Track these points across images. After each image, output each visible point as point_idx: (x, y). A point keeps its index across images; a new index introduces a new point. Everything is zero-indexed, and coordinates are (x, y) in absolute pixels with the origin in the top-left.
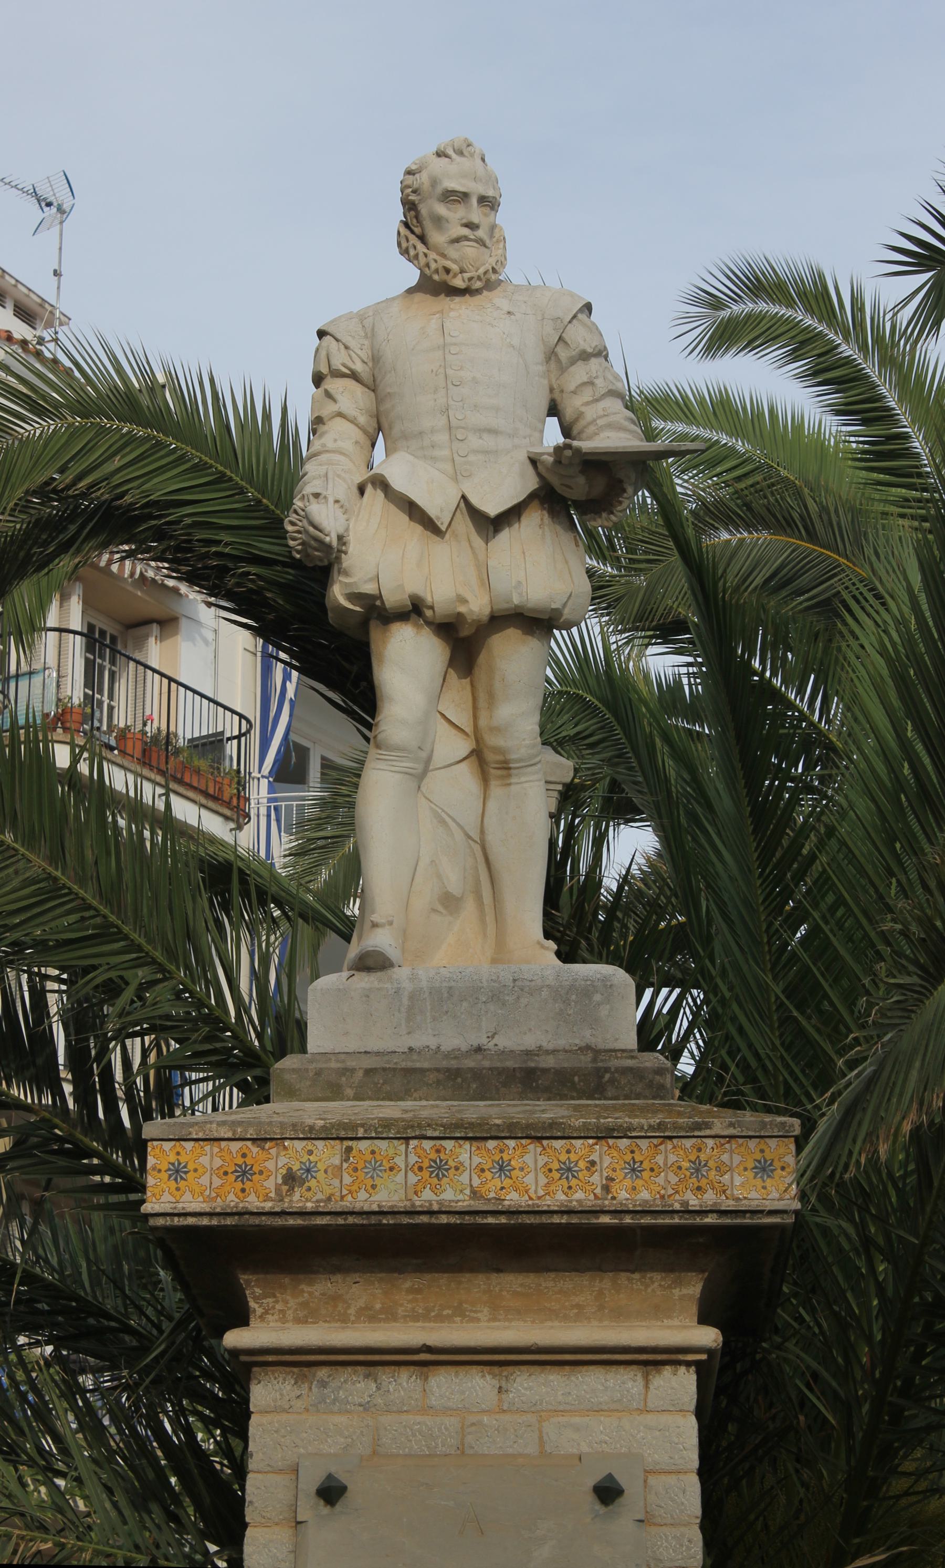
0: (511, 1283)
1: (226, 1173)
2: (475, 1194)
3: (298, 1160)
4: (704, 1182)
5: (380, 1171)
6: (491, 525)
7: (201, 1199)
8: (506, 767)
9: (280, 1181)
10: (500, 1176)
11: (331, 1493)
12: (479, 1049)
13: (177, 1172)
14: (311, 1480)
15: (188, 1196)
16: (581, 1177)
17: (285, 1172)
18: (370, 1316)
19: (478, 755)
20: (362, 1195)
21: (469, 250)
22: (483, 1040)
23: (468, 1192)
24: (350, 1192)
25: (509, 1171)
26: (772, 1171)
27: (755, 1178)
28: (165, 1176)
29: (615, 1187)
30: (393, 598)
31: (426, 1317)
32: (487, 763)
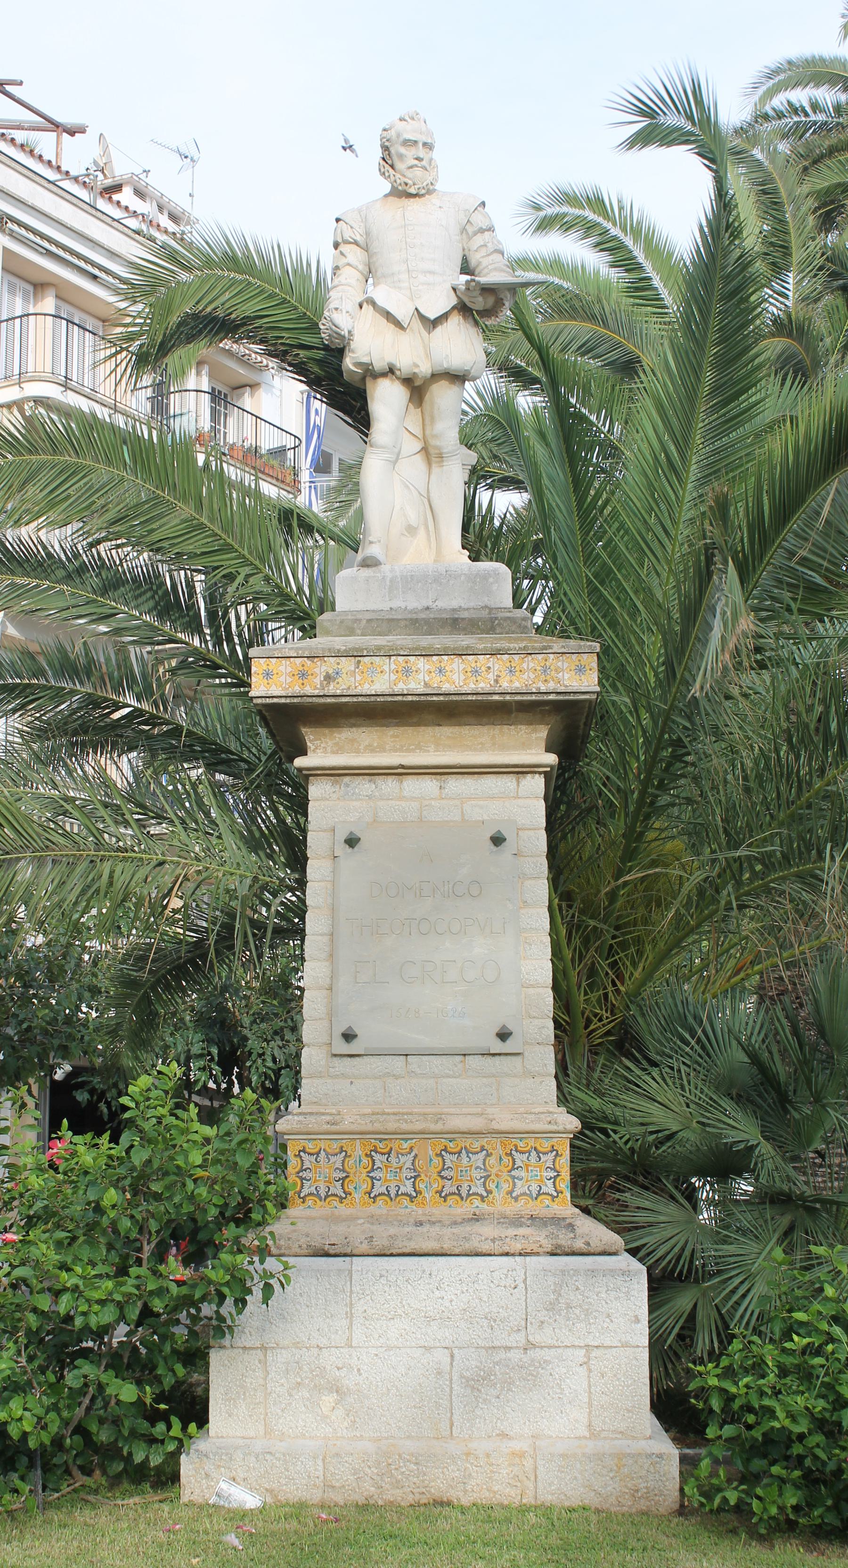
0: (447, 731)
4: (548, 677)
6: (433, 324)
8: (440, 456)
11: (352, 842)
12: (428, 608)
13: (268, 675)
14: (342, 835)
15: (274, 688)
18: (371, 749)
19: (425, 450)
20: (366, 686)
21: (418, 172)
22: (430, 604)
28: (261, 677)
29: (501, 681)
30: (379, 365)
31: (401, 750)
32: (430, 454)
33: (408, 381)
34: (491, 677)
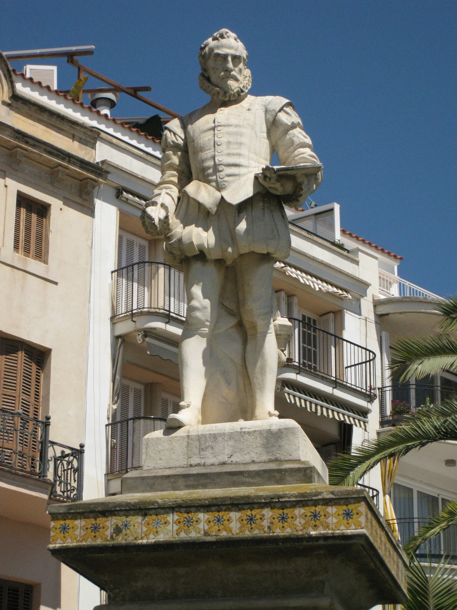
1: (87, 529)
2: (206, 534)
3: (121, 520)
4: (317, 523)
5: (160, 524)
7: (75, 541)
9: (112, 531)
10: (218, 524)
15: (69, 540)
16: (257, 523)
17: (115, 527)
20: (151, 536)
22: (226, 459)
23: (202, 532)
24: (146, 535)
25: (222, 521)
26: (352, 515)
27: (343, 519)
28: (58, 531)
29: (273, 527)
33: (220, 262)
34: (265, 523)
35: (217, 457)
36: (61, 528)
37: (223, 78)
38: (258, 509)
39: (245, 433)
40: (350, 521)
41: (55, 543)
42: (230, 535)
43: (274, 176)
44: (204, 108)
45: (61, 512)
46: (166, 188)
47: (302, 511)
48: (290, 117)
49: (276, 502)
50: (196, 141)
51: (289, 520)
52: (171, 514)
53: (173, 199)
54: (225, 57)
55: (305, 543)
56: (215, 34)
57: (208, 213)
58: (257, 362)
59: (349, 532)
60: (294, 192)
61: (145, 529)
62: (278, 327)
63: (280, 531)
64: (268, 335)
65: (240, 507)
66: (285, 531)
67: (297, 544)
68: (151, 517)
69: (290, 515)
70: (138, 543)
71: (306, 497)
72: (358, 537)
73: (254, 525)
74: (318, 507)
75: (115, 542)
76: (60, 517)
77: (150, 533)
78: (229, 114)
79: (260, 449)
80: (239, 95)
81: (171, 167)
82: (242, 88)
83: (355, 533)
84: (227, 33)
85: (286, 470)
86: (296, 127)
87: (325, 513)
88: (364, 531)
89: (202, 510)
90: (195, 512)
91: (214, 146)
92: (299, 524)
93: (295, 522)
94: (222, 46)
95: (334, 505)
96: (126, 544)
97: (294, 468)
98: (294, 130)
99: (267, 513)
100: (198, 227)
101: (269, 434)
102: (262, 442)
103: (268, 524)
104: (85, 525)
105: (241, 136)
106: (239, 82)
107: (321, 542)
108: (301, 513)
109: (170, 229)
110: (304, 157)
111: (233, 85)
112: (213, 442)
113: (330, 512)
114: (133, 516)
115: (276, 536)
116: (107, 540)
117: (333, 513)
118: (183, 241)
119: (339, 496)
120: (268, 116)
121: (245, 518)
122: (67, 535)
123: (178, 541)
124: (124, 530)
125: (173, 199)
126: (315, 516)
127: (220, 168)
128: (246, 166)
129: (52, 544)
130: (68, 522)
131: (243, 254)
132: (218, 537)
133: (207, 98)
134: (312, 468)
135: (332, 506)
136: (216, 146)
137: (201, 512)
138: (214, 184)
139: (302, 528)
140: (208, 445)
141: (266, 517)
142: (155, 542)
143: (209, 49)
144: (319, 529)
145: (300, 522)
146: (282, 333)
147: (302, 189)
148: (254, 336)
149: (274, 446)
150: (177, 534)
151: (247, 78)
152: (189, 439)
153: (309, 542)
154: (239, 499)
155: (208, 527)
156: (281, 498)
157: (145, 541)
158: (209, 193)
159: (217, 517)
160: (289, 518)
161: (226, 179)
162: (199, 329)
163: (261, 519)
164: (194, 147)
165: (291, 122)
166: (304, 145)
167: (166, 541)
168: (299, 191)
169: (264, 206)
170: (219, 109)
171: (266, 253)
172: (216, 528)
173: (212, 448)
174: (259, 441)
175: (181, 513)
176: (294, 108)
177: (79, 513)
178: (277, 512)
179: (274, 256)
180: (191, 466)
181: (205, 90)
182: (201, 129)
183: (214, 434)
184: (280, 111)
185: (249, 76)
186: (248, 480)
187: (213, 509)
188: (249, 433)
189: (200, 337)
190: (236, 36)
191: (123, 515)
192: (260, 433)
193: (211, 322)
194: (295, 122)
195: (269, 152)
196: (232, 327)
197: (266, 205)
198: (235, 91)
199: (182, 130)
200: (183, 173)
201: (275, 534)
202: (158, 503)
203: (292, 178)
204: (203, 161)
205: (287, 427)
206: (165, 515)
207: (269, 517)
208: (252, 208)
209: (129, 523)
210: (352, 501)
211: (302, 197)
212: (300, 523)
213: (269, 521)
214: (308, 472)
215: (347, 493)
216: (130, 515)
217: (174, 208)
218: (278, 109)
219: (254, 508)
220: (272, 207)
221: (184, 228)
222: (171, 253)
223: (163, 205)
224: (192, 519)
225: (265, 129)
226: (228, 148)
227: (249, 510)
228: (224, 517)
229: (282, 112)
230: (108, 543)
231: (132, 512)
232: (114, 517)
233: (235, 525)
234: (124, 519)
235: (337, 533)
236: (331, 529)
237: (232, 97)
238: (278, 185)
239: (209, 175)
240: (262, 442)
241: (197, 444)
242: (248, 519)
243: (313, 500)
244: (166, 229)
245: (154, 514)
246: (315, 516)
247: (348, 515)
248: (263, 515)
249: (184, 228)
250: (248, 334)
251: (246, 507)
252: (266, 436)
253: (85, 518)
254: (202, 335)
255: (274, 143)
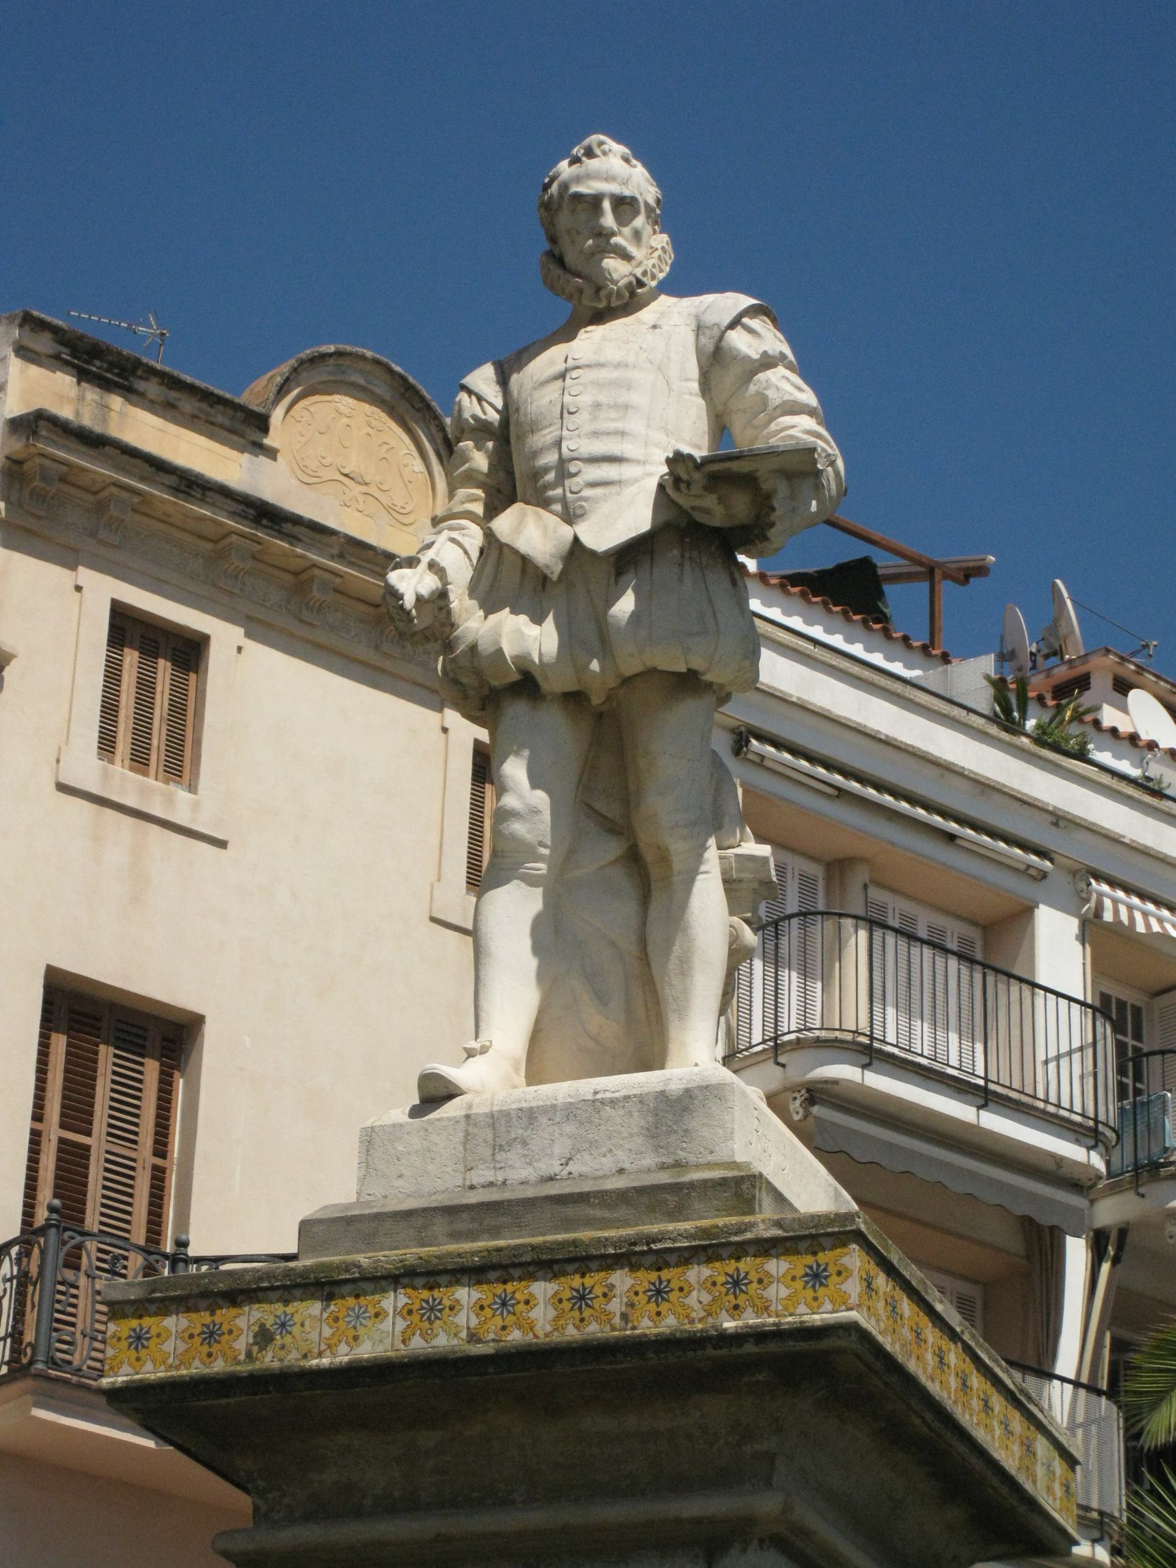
1: (191, 1336)
2: (473, 1337)
3: (272, 1313)
5: (365, 1318)
7: (163, 1368)
9: (251, 1341)
10: (502, 1313)
15: (149, 1366)
16: (596, 1306)
17: (256, 1328)
20: (343, 1348)
22: (557, 1169)
23: (464, 1334)
24: (329, 1347)
25: (513, 1306)
26: (826, 1278)
27: (804, 1288)
33: (575, 699)
34: (616, 1306)
35: (535, 1164)
36: (130, 1337)
37: (593, 254)
38: (598, 1271)
39: (603, 1102)
40: (821, 1291)
41: (116, 1375)
42: (529, 1337)
43: (697, 476)
44: (554, 334)
45: (132, 1297)
46: (451, 529)
47: (706, 1271)
48: (761, 339)
49: (643, 1253)
50: (522, 410)
51: (673, 1296)
52: (392, 1293)
53: (466, 552)
54: (595, 201)
55: (711, 1352)
56: (575, 151)
57: (543, 580)
58: (673, 944)
59: (817, 1319)
60: (758, 517)
61: (327, 1332)
62: (733, 860)
63: (651, 1324)
64: (700, 877)
65: (556, 1268)
66: (663, 1323)
67: (690, 1354)
68: (343, 1302)
69: (675, 1284)
70: (311, 1366)
71: (716, 1237)
72: (841, 1332)
73: (587, 1313)
74: (743, 1260)
75: (257, 1365)
76: (129, 1309)
77: (340, 1342)
78: (604, 338)
79: (639, 1140)
80: (633, 294)
81: (470, 478)
82: (639, 275)
83: (832, 1322)
84: (601, 144)
85: (692, 1185)
86: (775, 366)
87: (760, 1275)
88: (854, 1315)
89: (465, 1279)
90: (450, 1285)
91: (562, 417)
92: (697, 1306)
93: (687, 1301)
94: (589, 176)
95: (783, 1254)
96: (281, 1370)
97: (711, 1180)
98: (768, 372)
99: (621, 1279)
100: (517, 614)
101: (661, 1101)
102: (643, 1123)
103: (622, 1307)
104: (187, 1329)
105: (629, 387)
106: (634, 263)
107: (750, 1348)
108: (703, 1278)
109: (452, 625)
110: (792, 437)
111: (616, 270)
112: (526, 1129)
113: (774, 1272)
114: (302, 1300)
115: (638, 1336)
116: (239, 1363)
117: (781, 1274)
118: (480, 648)
119: (794, 1231)
120: (703, 340)
121: (567, 1294)
122: (143, 1353)
123: (405, 1357)
124: (278, 1337)
125: (466, 552)
126: (736, 1283)
127: (573, 468)
128: (638, 462)
129: (109, 1376)
130: (147, 1321)
131: (630, 678)
132: (502, 1344)
133: (565, 308)
134: (755, 1176)
135: (777, 1257)
136: (566, 414)
137: (464, 1286)
138: (558, 507)
139: (703, 1314)
140: (513, 1136)
141: (617, 1291)
142: (350, 1362)
143: (560, 186)
144: (744, 1315)
145: (696, 1300)
146: (743, 875)
147: (773, 509)
148: (667, 880)
149: (671, 1131)
150: (404, 1342)
151: (656, 254)
152: (469, 1124)
153: (721, 1348)
154: (552, 1250)
155: (477, 1321)
156: (654, 1242)
157: (325, 1362)
158: (545, 529)
159: (500, 1297)
160: (672, 1290)
161: (587, 492)
162: (520, 865)
163: (605, 1295)
164: (518, 424)
165: (761, 351)
166: (795, 408)
167: (375, 1358)
168: (768, 515)
169: (683, 556)
170: (583, 330)
171: (684, 670)
172: (498, 1321)
173: (524, 1143)
174: (637, 1121)
175: (415, 1288)
176: (774, 321)
177: (172, 1299)
178: (646, 1278)
179: (708, 677)
180: (472, 1187)
181: (552, 288)
182: (535, 378)
183: (531, 1109)
184: (732, 325)
185: (663, 248)
186: (598, 1213)
187: (492, 1275)
188: (613, 1102)
189: (523, 885)
190: (627, 151)
191: (278, 1301)
192: (641, 1102)
193: (553, 848)
194: (770, 352)
195: (706, 428)
196: (613, 863)
197: (687, 555)
198: (621, 283)
199: (498, 388)
200: (499, 491)
201: (638, 1332)
202: (360, 1267)
203: (748, 481)
204: (535, 454)
205: (705, 1084)
206: (377, 1297)
207: (626, 1289)
208: (652, 559)
209: (291, 1319)
210: (827, 1242)
211: (773, 530)
212: (700, 1302)
213: (625, 1300)
214: (744, 1187)
215: (816, 1221)
216: (295, 1299)
217: (468, 573)
218: (726, 321)
219: (590, 1271)
220: (704, 559)
221: (486, 618)
222: (456, 682)
223: (433, 566)
224: (440, 1303)
225: (694, 371)
226: (594, 418)
227: (577, 1276)
228: (517, 1296)
229: (739, 328)
230: (238, 1368)
231: (298, 1293)
232: (257, 1306)
233: (542, 1314)
234: (279, 1308)
235: (788, 1323)
236: (773, 1314)
237: (613, 299)
238: (710, 501)
239: (546, 487)
240: (643, 1123)
241: (488, 1134)
242: (574, 1298)
243: (730, 1244)
244: (443, 625)
245: (350, 1295)
246: (736, 1283)
247: (816, 1277)
248: (612, 1287)
249: (486, 618)
250: (653, 878)
251: (570, 1268)
252: (655, 1109)
253: (188, 1310)
254: (532, 881)
255: (720, 408)
